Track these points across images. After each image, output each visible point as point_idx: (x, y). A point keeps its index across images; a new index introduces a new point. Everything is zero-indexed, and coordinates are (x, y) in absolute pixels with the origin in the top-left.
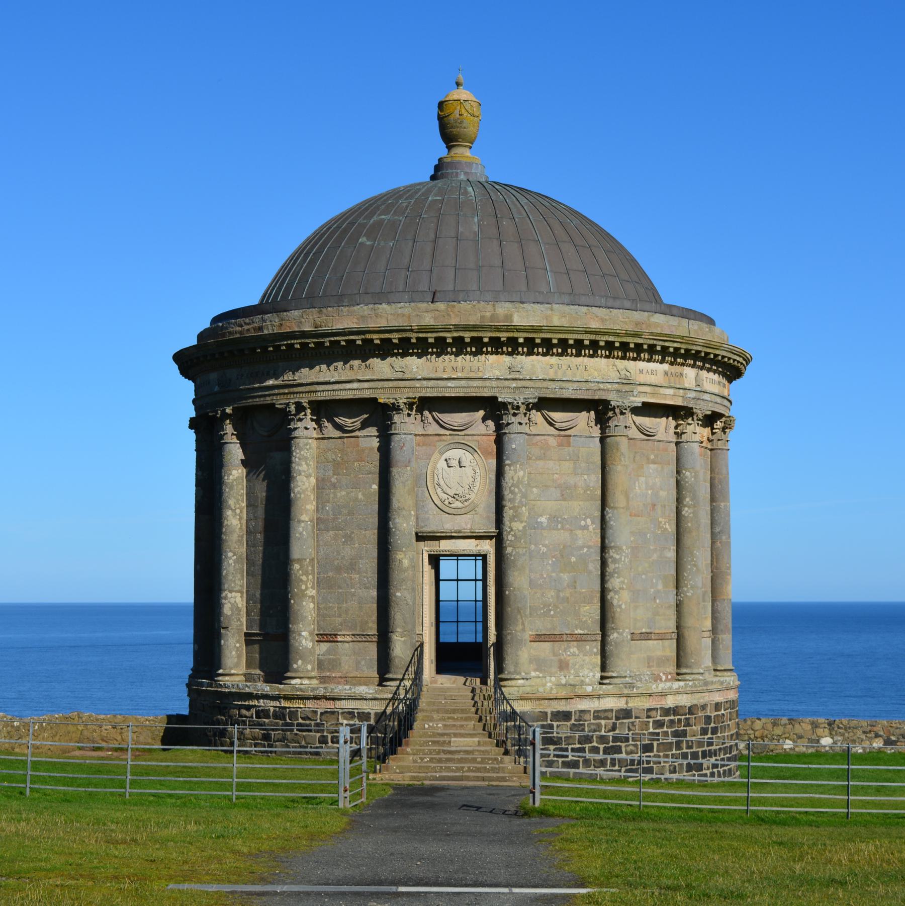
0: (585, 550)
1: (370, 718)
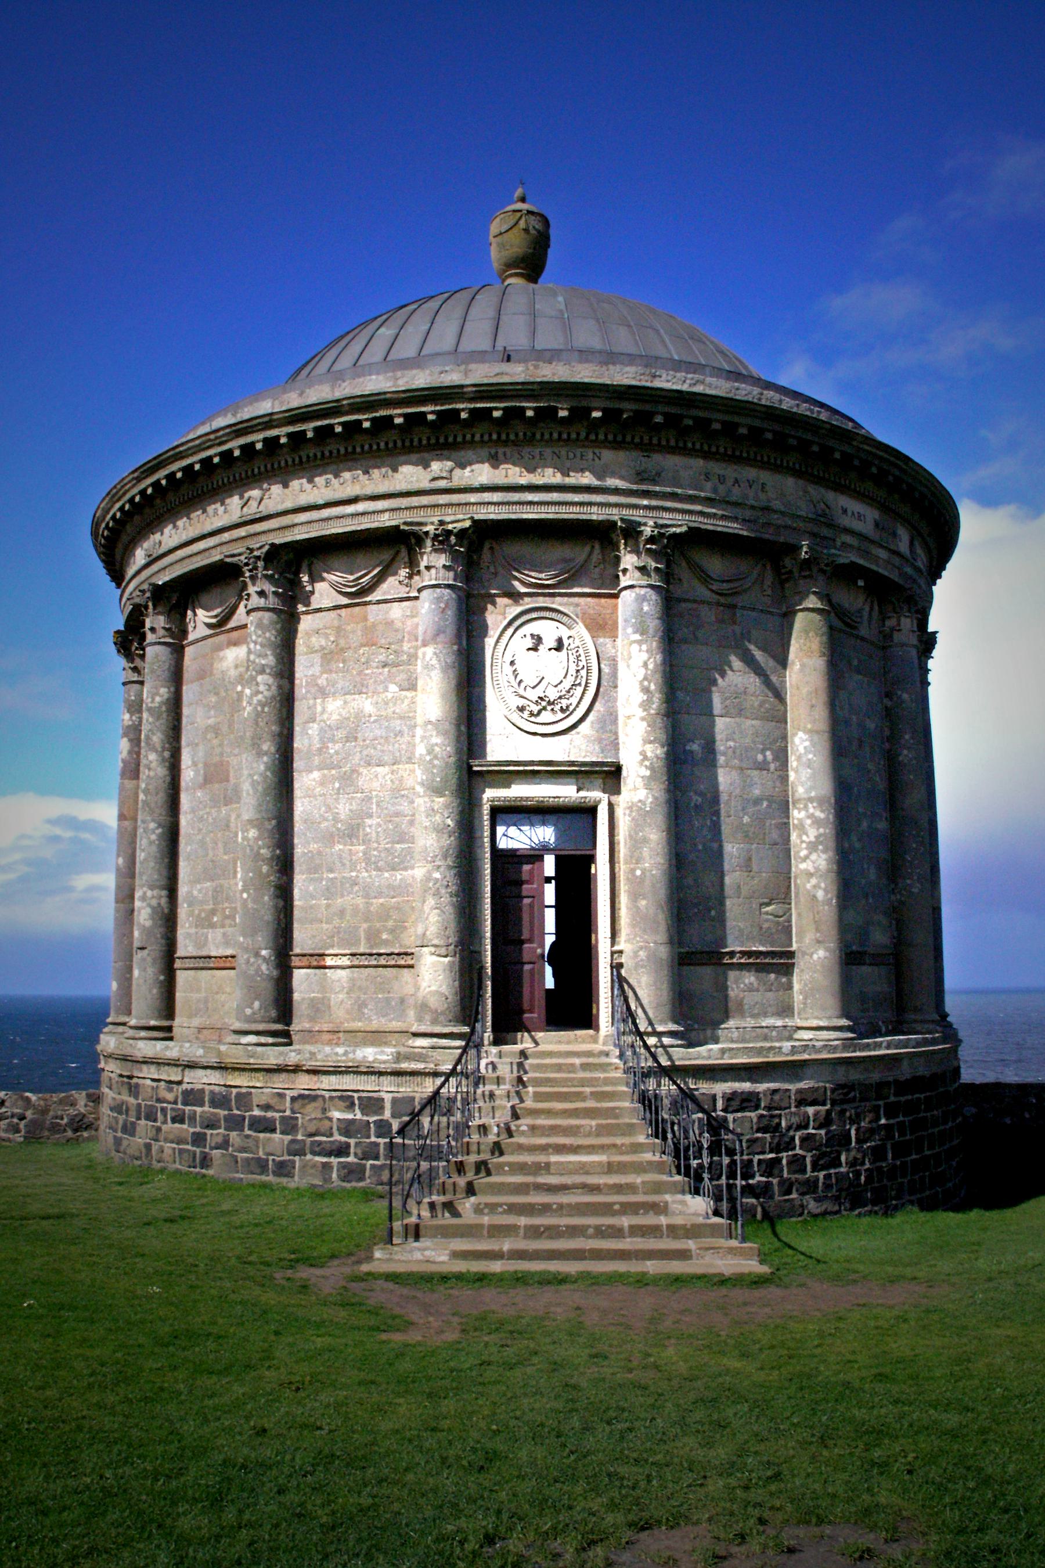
0: (765, 804)
1: (382, 1108)
